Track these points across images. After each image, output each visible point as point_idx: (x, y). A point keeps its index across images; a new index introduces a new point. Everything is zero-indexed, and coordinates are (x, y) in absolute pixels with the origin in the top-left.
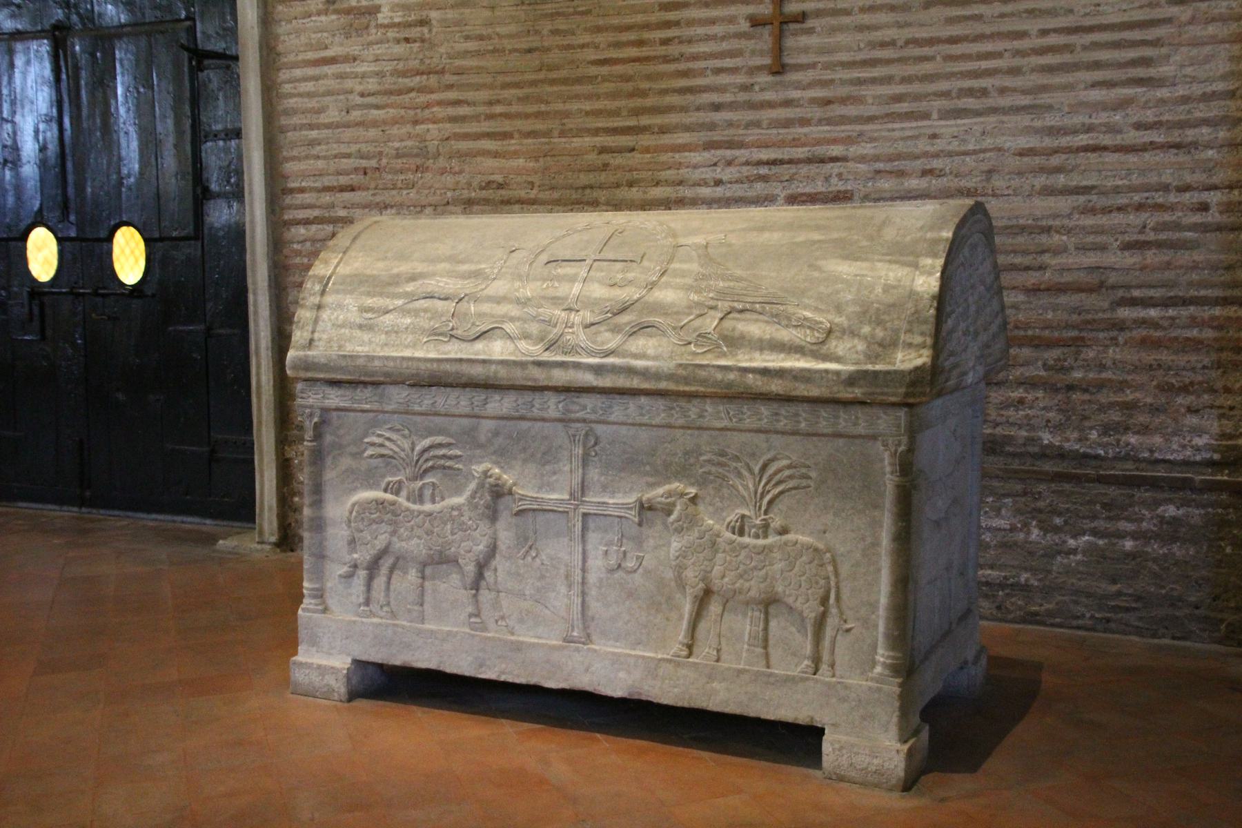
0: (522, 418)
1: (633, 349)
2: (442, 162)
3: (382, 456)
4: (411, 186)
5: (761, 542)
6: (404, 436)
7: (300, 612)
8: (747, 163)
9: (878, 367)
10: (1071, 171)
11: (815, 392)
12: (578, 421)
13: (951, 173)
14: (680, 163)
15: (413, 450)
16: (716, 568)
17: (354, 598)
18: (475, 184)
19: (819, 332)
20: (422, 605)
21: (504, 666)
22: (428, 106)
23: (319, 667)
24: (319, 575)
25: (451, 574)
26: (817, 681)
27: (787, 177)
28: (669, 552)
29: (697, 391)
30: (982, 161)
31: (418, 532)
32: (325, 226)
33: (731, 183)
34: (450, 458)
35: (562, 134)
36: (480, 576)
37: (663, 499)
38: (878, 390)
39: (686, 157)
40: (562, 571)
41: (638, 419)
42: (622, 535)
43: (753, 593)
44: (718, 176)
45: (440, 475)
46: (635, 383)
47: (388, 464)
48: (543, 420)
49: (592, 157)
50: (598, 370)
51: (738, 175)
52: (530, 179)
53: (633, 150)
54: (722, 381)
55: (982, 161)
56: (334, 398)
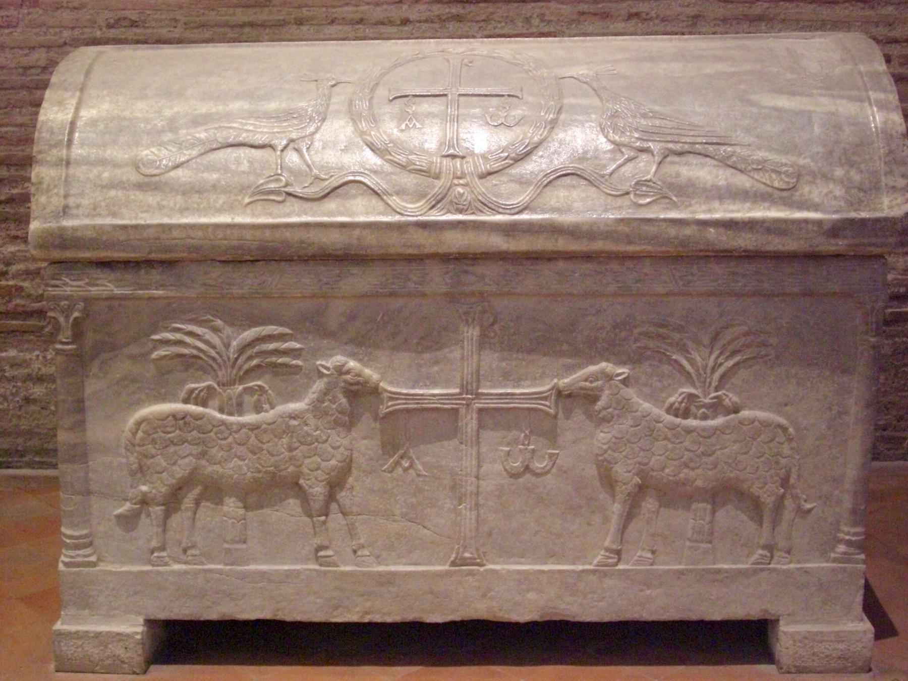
0: (393, 295)
1: (553, 203)
3: (182, 356)
6: (215, 330)
7: (61, 567)
9: (864, 215)
10: (772, 20)
13: (658, 16)
18: (101, 21)
19: (788, 176)
21: (368, 604)
23: (98, 635)
25: (287, 498)
27: (484, 17)
29: (642, 251)
31: (241, 450)
33: (420, 22)
34: (285, 353)
36: (331, 497)
37: (587, 384)
38: (866, 241)
44: (404, 15)
45: (268, 377)
46: (562, 244)
50: (510, 229)
54: (676, 238)
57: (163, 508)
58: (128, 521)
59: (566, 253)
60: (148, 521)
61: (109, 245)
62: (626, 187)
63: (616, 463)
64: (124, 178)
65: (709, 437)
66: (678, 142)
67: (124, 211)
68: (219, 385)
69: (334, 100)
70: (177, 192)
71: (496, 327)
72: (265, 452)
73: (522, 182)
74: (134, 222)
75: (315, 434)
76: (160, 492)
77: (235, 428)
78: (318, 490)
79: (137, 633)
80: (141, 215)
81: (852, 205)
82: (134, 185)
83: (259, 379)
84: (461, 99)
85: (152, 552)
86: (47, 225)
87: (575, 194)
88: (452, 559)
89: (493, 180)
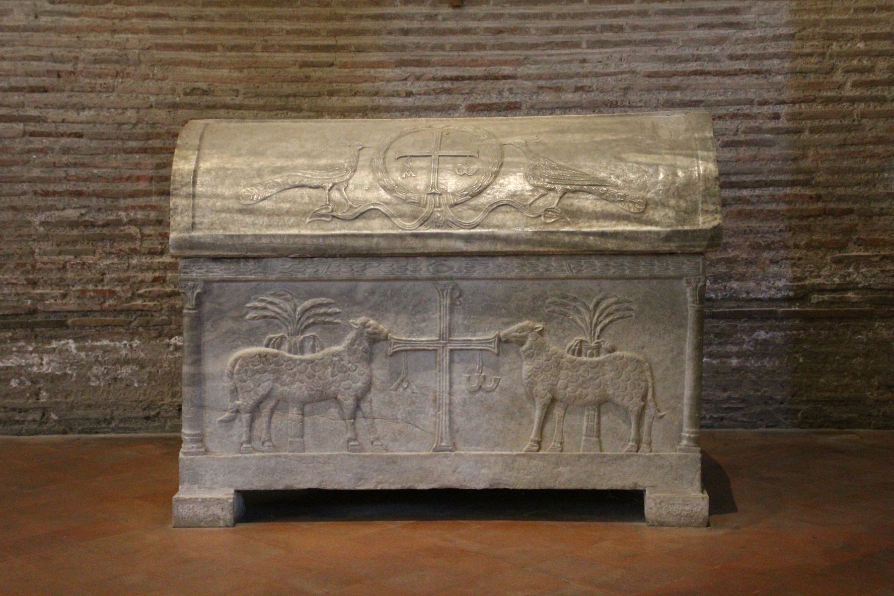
0: (397, 279)
1: (495, 222)
2: (143, 69)
3: (265, 317)
4: (110, 89)
5: (595, 359)
6: (287, 300)
7: (181, 455)
8: (434, 79)
9: (687, 228)
11: (642, 247)
12: (446, 278)
13: (597, 89)
14: (375, 78)
15: (295, 311)
16: (560, 382)
17: (235, 438)
18: (179, 89)
19: (639, 205)
20: (302, 437)
21: (381, 477)
22: (127, 17)
23: (204, 500)
24: (198, 421)
25: (330, 408)
26: (640, 456)
27: (467, 91)
28: (521, 373)
30: (620, 81)
32: (14, 125)
33: (420, 94)
35: (265, 49)
36: (358, 407)
38: (687, 244)
39: (380, 72)
40: (431, 397)
41: (496, 275)
42: (483, 364)
43: (589, 398)
44: (409, 89)
45: (319, 330)
46: (499, 247)
47: (270, 323)
48: (416, 279)
49: (294, 70)
50: (468, 238)
51: (426, 88)
52: (235, 87)
53: (331, 65)
54: (569, 243)
55: (620, 81)
56: (218, 272)
59: (503, 252)
60: (240, 424)
61: (222, 247)
62: (539, 213)
64: (231, 206)
66: (573, 185)
67: (231, 226)
69: (361, 159)
70: (264, 215)
71: (461, 299)
73: (476, 209)
74: (237, 233)
78: (350, 402)
79: (230, 498)
80: (242, 229)
81: (679, 222)
82: (237, 211)
84: (441, 158)
86: (182, 235)
87: (508, 216)
88: (434, 446)
89: (458, 208)
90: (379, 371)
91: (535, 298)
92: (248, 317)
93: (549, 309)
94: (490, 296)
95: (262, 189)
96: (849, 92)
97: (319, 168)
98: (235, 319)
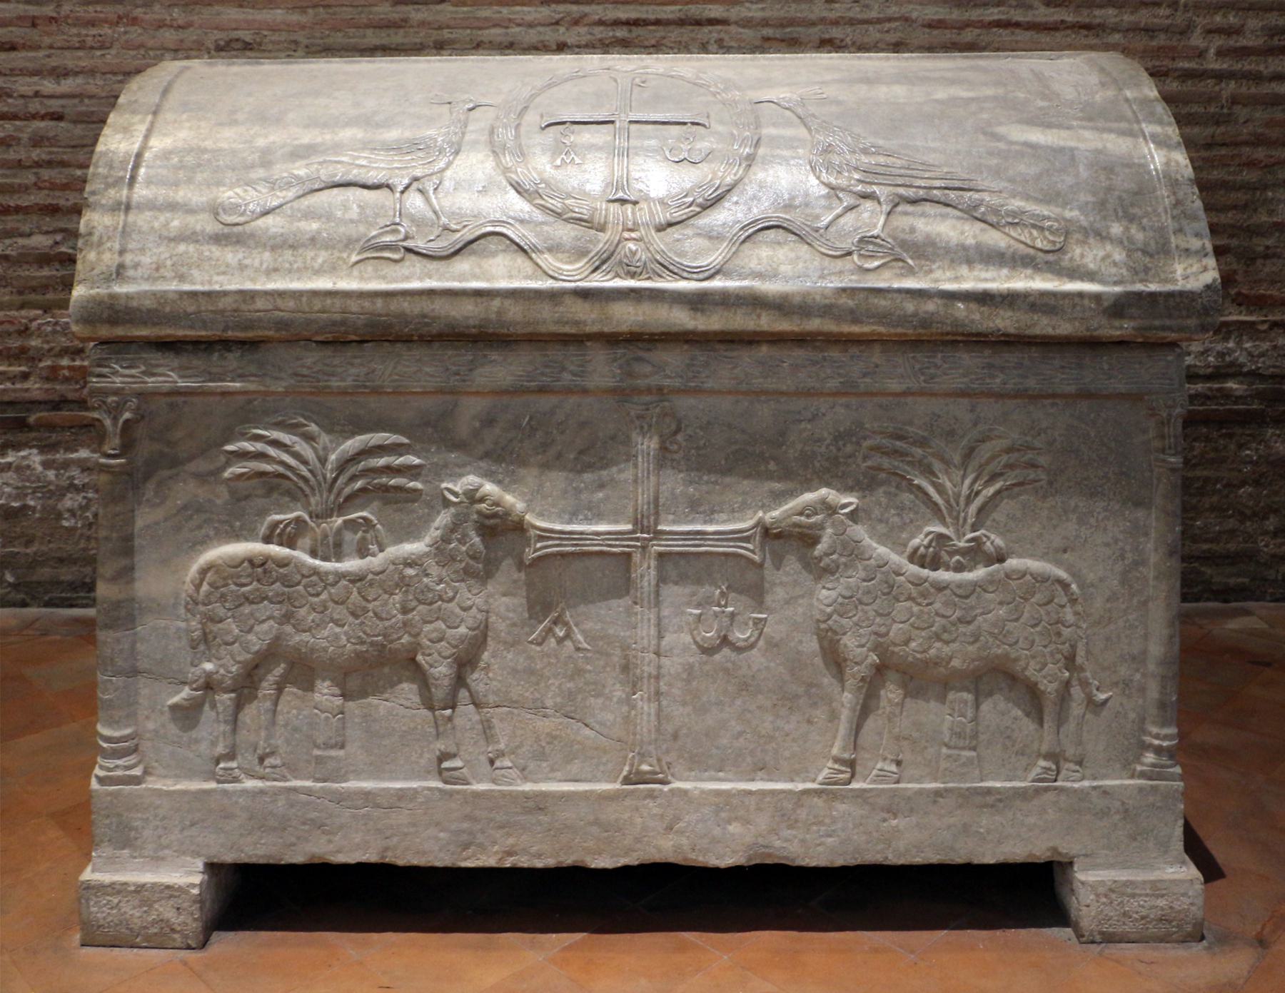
1: (753, 264)
8: (601, 23)
9: (1153, 287)
11: (1065, 328)
14: (510, 20)
27: (653, 42)
29: (872, 333)
30: (888, 32)
38: (1157, 323)
39: (518, 12)
41: (758, 382)
44: (562, 39)
46: (766, 322)
48: (585, 391)
50: (697, 301)
51: (589, 37)
54: (915, 315)
55: (888, 32)
57: (233, 695)
58: (187, 715)
59: (772, 334)
61: (174, 319)
62: (847, 245)
63: (844, 634)
64: (198, 228)
65: (967, 597)
66: (911, 186)
67: (195, 272)
68: (311, 517)
69: (470, 128)
70: (265, 245)
72: (371, 614)
73: (714, 237)
74: (206, 288)
75: (438, 588)
76: (230, 672)
77: (331, 578)
80: (216, 278)
81: (1136, 273)
82: (210, 238)
83: (362, 508)
84: (633, 127)
85: (218, 763)
86: (93, 292)
87: (782, 253)
89: (674, 233)
90: (504, 599)
91: (839, 437)
92: (226, 474)
93: (869, 463)
94: (743, 431)
95: (264, 191)
96: (1213, 64)
97: (389, 148)
98: (202, 478)
